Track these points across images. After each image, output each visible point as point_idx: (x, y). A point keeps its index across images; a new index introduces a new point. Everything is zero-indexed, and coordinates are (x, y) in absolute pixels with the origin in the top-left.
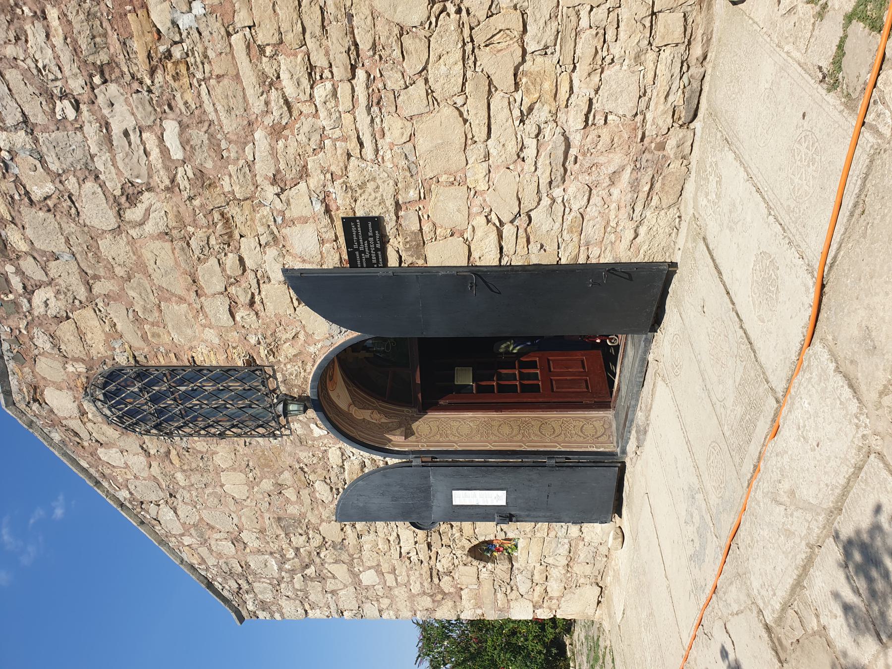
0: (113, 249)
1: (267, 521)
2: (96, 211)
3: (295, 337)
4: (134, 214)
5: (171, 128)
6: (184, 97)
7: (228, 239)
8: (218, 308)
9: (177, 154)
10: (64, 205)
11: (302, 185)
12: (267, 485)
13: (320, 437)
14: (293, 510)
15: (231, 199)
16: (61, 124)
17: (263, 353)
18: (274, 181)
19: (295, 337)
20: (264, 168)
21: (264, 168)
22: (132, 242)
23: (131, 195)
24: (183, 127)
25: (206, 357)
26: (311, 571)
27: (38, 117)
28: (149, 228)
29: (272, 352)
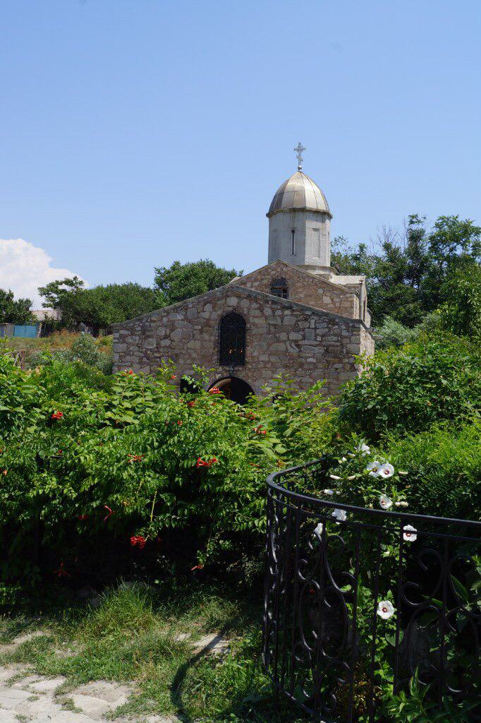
0: (283, 336)
1: (176, 351)
2: (293, 336)
3: (254, 376)
4: (293, 345)
5: (314, 361)
6: (320, 365)
7: (286, 367)
8: (264, 358)
9: (309, 360)
10: (296, 328)
11: (298, 387)
12: (194, 355)
13: (215, 376)
14: (181, 361)
15: (296, 370)
16: (316, 336)
17: (250, 367)
18: (300, 381)
19: (254, 376)
20: (304, 380)
21: (304, 380)
22: (284, 342)
23: (298, 346)
24: (314, 364)
25: (249, 350)
26: (145, 359)
27: (318, 331)
28: (289, 347)
29: (249, 369)
